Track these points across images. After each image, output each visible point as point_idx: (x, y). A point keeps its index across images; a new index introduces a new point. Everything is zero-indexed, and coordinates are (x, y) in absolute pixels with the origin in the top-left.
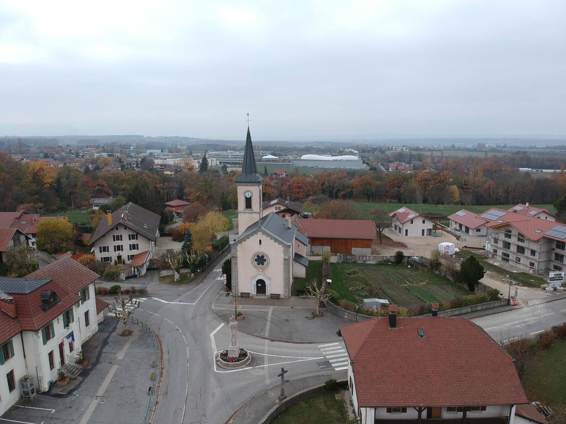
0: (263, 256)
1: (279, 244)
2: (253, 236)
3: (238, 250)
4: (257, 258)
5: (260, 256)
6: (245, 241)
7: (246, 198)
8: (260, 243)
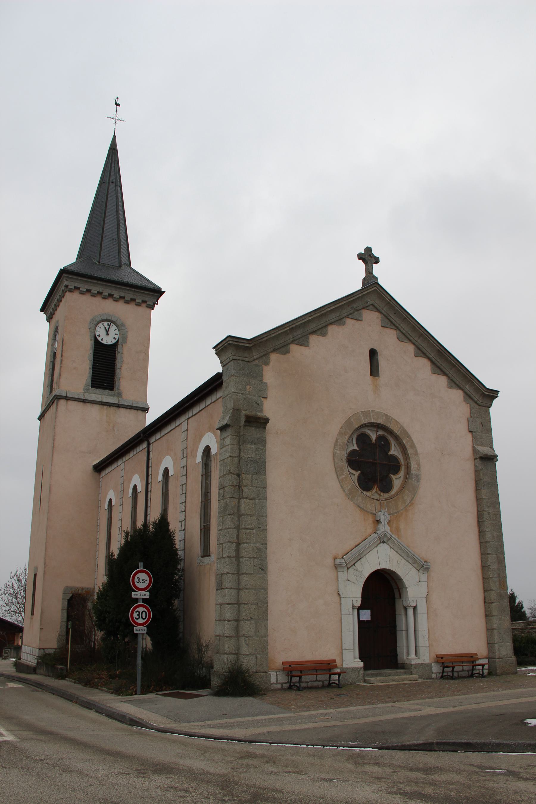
1: (453, 384)
2: (340, 321)
3: (266, 384)
4: (356, 448)
6: (303, 342)
7: (98, 345)
8: (374, 370)
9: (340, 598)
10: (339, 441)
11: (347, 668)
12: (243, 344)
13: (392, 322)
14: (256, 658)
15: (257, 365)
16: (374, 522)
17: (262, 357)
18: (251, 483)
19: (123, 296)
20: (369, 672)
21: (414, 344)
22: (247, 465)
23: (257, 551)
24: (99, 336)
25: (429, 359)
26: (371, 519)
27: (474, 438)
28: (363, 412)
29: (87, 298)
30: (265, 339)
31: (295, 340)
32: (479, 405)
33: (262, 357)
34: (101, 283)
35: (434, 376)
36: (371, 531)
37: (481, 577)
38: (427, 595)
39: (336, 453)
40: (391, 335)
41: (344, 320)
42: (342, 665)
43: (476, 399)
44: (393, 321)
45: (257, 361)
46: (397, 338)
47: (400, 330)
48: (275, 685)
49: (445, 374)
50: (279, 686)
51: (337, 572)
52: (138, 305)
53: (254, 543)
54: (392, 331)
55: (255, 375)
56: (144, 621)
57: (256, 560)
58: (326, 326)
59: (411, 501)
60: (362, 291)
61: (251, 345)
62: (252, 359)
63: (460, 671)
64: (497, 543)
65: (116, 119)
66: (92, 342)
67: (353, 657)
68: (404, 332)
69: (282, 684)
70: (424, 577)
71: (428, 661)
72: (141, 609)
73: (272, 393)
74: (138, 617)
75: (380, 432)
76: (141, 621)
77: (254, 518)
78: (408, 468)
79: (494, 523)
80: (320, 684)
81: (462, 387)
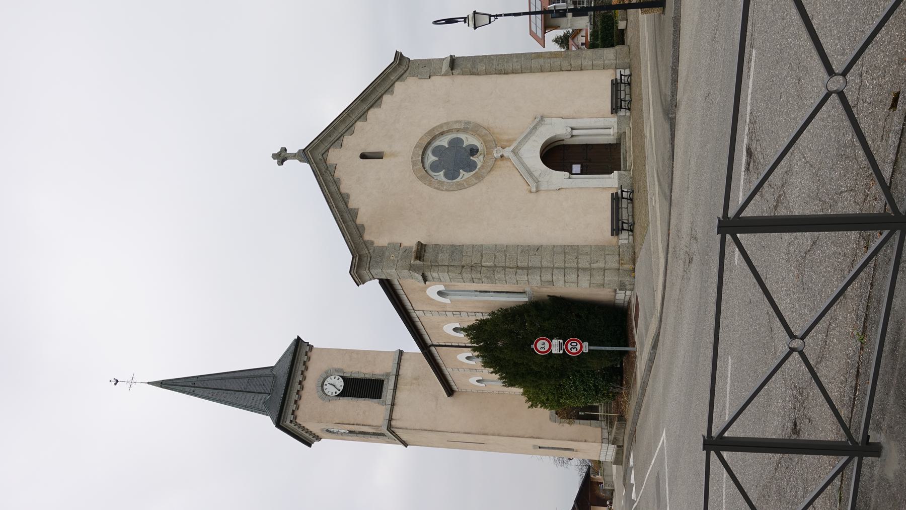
0: (452, 175)
1: (389, 90)
2: (337, 183)
4: (442, 173)
5: (434, 162)
6: (354, 213)
7: (344, 394)
8: (378, 156)
9: (562, 188)
10: (436, 186)
11: (619, 184)
12: (357, 262)
13: (337, 140)
14: (608, 254)
15: (374, 251)
16: (503, 160)
17: (367, 247)
18: (469, 256)
19: (301, 372)
20: (622, 166)
21: (356, 122)
22: (455, 260)
23: (523, 253)
24: (336, 393)
25: (369, 109)
26: (500, 163)
27: (435, 74)
28: (413, 166)
29: (302, 403)
30: (352, 243)
31: (353, 220)
32: (408, 68)
33: (367, 247)
34: (289, 391)
35: (382, 106)
36: (509, 162)
37: (550, 73)
38: (562, 118)
39: (446, 189)
40: (348, 140)
41: (335, 179)
42: (616, 188)
43: (403, 71)
44: (336, 138)
45: (370, 251)
46: (351, 135)
47: (344, 133)
48: (630, 241)
49: (381, 97)
50: (631, 237)
51: (541, 190)
52: (309, 359)
53: (517, 256)
54: (345, 139)
55: (382, 252)
56: (578, 343)
57: (531, 254)
58: (341, 194)
59: (486, 130)
60: (311, 163)
61: (358, 255)
62: (369, 254)
63: (625, 92)
64: (523, 59)
65: (131, 382)
66: (341, 398)
67: (610, 179)
68: (346, 129)
69: (629, 235)
70: (547, 120)
71: (615, 119)
72: (569, 347)
73: (397, 239)
74: (575, 349)
75: (429, 152)
76: (578, 347)
77: (497, 254)
78: (458, 130)
79: (506, 60)
80: (630, 205)
81: (392, 83)
